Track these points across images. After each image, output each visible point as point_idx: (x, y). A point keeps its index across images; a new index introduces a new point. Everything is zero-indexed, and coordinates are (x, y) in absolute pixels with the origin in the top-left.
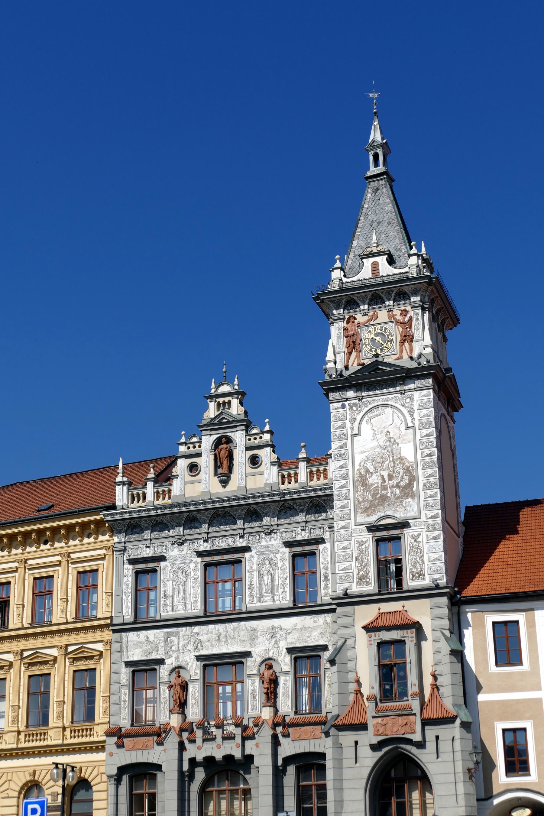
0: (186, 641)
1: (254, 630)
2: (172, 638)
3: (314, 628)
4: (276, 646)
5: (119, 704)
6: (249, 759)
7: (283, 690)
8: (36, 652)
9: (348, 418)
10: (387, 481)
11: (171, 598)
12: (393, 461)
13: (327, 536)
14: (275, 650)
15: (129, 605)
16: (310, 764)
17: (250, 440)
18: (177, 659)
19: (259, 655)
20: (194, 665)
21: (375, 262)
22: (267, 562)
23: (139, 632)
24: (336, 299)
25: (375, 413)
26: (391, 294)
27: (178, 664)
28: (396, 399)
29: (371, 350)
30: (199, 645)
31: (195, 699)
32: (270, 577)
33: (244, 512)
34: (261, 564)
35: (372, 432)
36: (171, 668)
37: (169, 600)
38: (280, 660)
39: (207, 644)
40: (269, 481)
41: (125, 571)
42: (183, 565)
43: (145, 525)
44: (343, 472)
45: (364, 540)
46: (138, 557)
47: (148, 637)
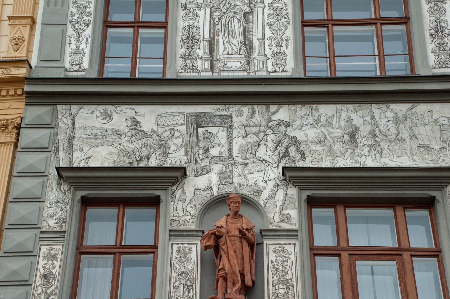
0: (252, 139)
2: (209, 129)
5: (25, 283)
11: (207, 45)
18: (225, 177)
23: (110, 108)
27: (229, 189)
30: (292, 151)
36: (206, 196)
39: (319, 148)
47: (137, 123)
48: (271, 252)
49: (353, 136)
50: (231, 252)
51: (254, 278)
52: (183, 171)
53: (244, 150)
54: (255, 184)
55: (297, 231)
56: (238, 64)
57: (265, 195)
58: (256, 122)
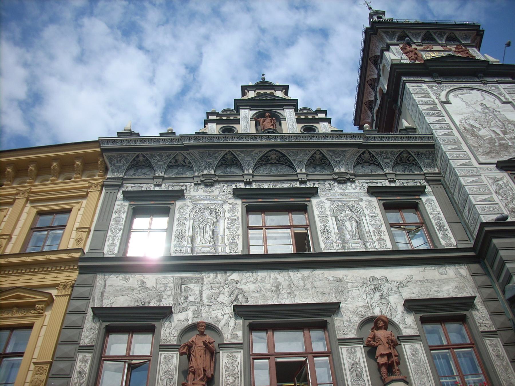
1: (340, 280)
4: (384, 301)
5: (68, 376)
7: (412, 365)
12: (500, 121)
13: (428, 189)
14: (384, 307)
18: (197, 313)
19: (354, 313)
20: (232, 323)
22: (346, 209)
24: (390, 30)
26: (442, 36)
27: (199, 320)
30: (240, 297)
32: (354, 224)
33: (307, 158)
35: (464, 103)
36: (185, 324)
38: (396, 319)
39: (257, 295)
41: (116, 208)
42: (213, 206)
43: (159, 163)
47: (144, 283)
48: (225, 358)
49: (278, 287)
50: (198, 356)
51: (212, 372)
53: (210, 298)
54: (216, 317)
55: (241, 344)
56: (209, 249)
58: (218, 281)
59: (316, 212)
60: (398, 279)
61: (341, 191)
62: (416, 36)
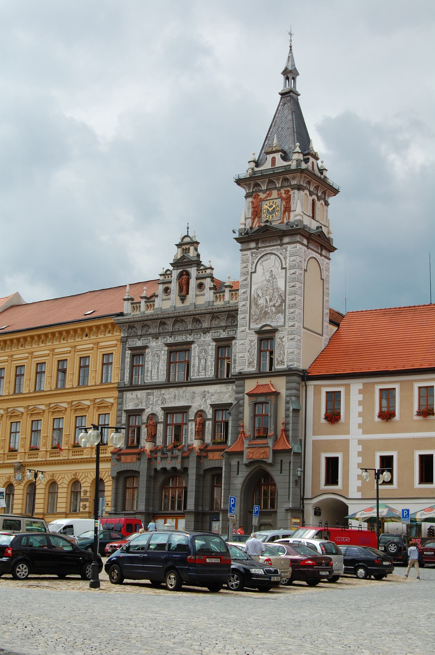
0: (157, 399)
1: (194, 393)
3: (226, 393)
6: (185, 470)
8: (35, 408)
9: (250, 261)
10: (268, 302)
14: (204, 405)
15: (128, 375)
16: (215, 474)
17: (199, 273)
18: (152, 409)
21: (274, 157)
22: (203, 351)
23: (133, 392)
25: (265, 258)
26: (279, 180)
27: (152, 412)
28: (278, 249)
29: (266, 217)
31: (160, 433)
32: (204, 360)
33: (191, 320)
34: (201, 352)
35: (263, 271)
36: (149, 414)
37: (150, 372)
38: (207, 411)
40: (208, 300)
42: (158, 352)
44: (245, 296)
45: (253, 339)
46: (134, 346)
52: (144, 409)
57: (159, 413)
59: (192, 354)
60: (212, 392)
61: (203, 339)
62: (264, 182)
